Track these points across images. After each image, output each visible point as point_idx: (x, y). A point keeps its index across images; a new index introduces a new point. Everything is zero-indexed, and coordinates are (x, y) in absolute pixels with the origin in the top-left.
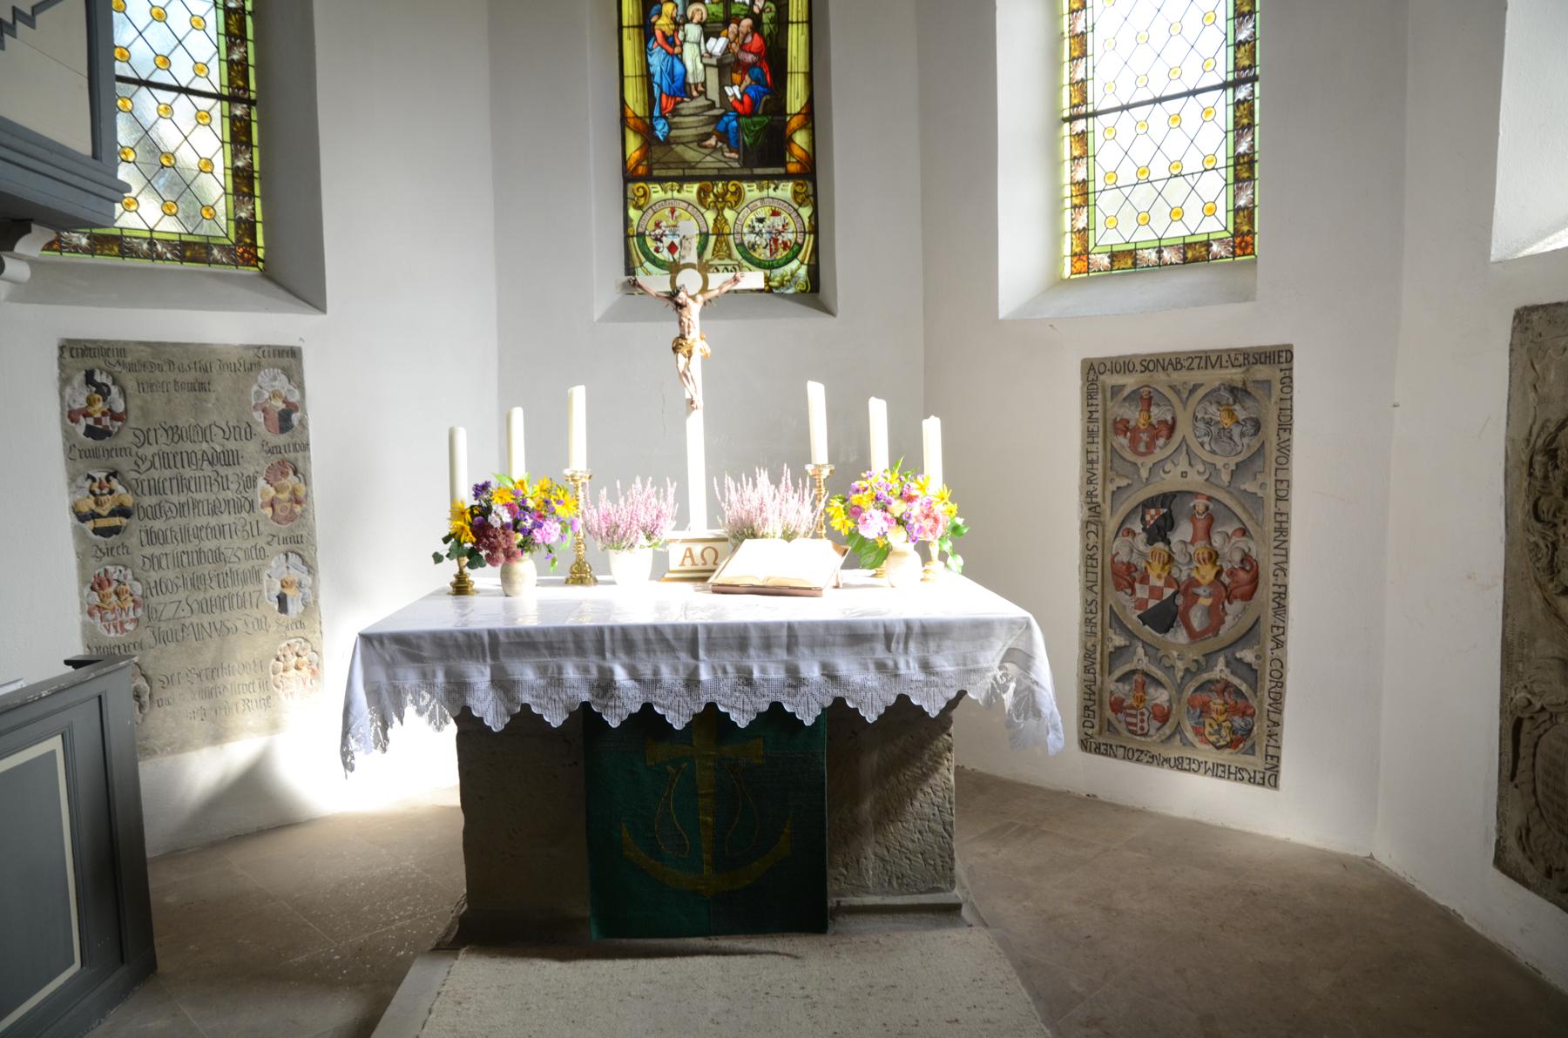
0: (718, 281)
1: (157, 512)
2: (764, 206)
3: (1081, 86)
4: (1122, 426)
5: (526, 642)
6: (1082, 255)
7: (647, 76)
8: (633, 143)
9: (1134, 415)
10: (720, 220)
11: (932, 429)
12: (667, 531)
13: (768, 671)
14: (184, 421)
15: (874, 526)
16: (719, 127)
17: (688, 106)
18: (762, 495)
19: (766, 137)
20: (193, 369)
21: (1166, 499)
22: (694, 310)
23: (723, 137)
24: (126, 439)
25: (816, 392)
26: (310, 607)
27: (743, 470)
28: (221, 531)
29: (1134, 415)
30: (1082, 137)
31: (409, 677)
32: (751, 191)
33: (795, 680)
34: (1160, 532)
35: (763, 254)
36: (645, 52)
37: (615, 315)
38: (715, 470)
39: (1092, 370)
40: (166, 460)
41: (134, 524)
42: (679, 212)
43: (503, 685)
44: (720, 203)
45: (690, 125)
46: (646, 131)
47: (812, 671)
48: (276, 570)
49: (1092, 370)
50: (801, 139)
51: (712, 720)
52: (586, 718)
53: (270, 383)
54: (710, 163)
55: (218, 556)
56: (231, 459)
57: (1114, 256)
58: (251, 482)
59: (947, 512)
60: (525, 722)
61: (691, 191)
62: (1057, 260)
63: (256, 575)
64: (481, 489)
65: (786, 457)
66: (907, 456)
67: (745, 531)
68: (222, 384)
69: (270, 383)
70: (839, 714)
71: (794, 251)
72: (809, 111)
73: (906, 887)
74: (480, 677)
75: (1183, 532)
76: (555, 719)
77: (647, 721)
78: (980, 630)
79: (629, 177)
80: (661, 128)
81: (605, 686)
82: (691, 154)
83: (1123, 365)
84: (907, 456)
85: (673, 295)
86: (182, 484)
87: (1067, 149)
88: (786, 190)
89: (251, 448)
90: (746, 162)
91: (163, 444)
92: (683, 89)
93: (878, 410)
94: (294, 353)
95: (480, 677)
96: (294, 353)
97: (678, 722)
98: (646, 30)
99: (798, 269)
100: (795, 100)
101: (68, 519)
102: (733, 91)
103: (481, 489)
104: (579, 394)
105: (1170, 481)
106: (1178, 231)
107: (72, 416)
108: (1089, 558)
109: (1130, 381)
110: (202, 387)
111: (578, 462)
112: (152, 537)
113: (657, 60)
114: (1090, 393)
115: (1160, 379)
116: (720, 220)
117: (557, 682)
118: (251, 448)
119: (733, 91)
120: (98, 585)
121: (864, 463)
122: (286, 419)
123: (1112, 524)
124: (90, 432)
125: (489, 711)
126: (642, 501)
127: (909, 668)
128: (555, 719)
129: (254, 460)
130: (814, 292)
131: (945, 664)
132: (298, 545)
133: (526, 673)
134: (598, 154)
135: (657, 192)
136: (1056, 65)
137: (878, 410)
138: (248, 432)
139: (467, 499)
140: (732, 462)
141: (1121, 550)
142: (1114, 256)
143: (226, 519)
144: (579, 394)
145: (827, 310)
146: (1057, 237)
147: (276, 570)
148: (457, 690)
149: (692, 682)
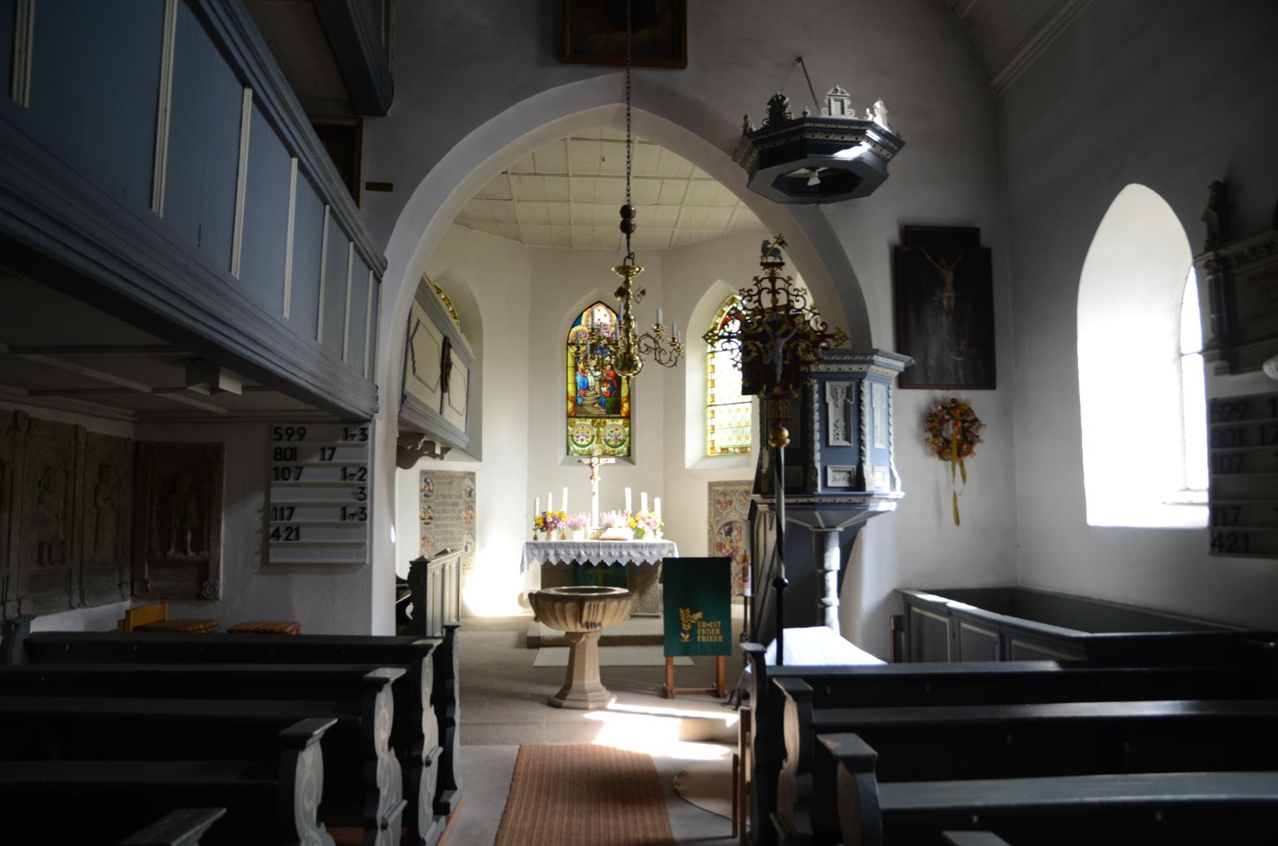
0: (603, 460)
1: (438, 519)
2: (615, 426)
3: (713, 396)
4: (719, 502)
5: (562, 545)
6: (713, 448)
7: (576, 383)
8: (570, 405)
9: (721, 498)
10: (598, 432)
11: (657, 502)
12: (588, 526)
13: (615, 553)
14: (446, 493)
15: (641, 525)
16: (599, 401)
17: (589, 393)
18: (613, 517)
19: (614, 406)
20: (449, 478)
21: (730, 523)
22: (596, 469)
23: (600, 404)
24: (433, 498)
25: (628, 491)
26: (473, 550)
27: (608, 511)
28: (452, 526)
29: (721, 498)
30: (713, 412)
31: (536, 552)
32: (609, 422)
33: (621, 555)
34: (729, 533)
35: (612, 443)
36: (575, 375)
37: (564, 463)
38: (601, 510)
39: (711, 485)
40: (441, 504)
41: (433, 522)
42: (583, 427)
43: (557, 555)
44: (599, 425)
45: (590, 398)
46: (575, 402)
47: (625, 553)
48: (466, 538)
49: (711, 485)
50: (626, 406)
51: (602, 564)
52: (575, 563)
53: (467, 482)
54: (595, 412)
55: (452, 533)
56: (456, 504)
57: (722, 449)
58: (460, 512)
59: (659, 521)
60: (561, 563)
61: (589, 421)
62: (705, 449)
63: (460, 539)
64: (544, 513)
65: (620, 507)
66: (651, 508)
67: (608, 526)
68: (456, 482)
69: (467, 482)
70: (631, 563)
71: (623, 442)
72: (629, 397)
73: (646, 610)
74: (552, 552)
75: (734, 533)
76: (568, 563)
77: (588, 564)
78: (663, 546)
79: (569, 416)
80: (580, 401)
81: (579, 555)
82: (589, 409)
83: (718, 484)
84: (651, 508)
85: (591, 465)
86: (445, 511)
87: (709, 415)
88: (621, 422)
89: (461, 502)
90: (608, 412)
91: (441, 500)
92: (587, 388)
93: (644, 496)
94: (473, 474)
95: (552, 552)
96: (473, 474)
97: (595, 564)
98: (576, 368)
99: (624, 448)
100: (624, 393)
101: (418, 520)
102: (604, 389)
103: (544, 513)
104: (565, 490)
105: (731, 517)
106: (739, 443)
107: (422, 490)
108: (710, 541)
109: (721, 489)
110: (450, 483)
111: (564, 508)
112: (437, 526)
113: (579, 378)
114: (710, 492)
115: (728, 489)
116: (598, 432)
117: (569, 554)
118: (461, 502)
119: (604, 389)
120: (424, 538)
121: (640, 509)
122: (470, 493)
123: (716, 531)
124: (426, 496)
125: (553, 561)
126: (581, 517)
127: (646, 553)
128: (568, 563)
129: (462, 506)
130: (629, 457)
131: (655, 553)
132: (472, 532)
133: (562, 552)
134: (561, 407)
135: (578, 421)
136: (705, 389)
137: (644, 496)
138: (460, 496)
139: (538, 514)
140: (605, 508)
141: (718, 539)
142: (722, 449)
143: (454, 522)
144: (565, 490)
145: (633, 463)
146: (705, 442)
147: (466, 538)
148: (547, 555)
149: (598, 555)
